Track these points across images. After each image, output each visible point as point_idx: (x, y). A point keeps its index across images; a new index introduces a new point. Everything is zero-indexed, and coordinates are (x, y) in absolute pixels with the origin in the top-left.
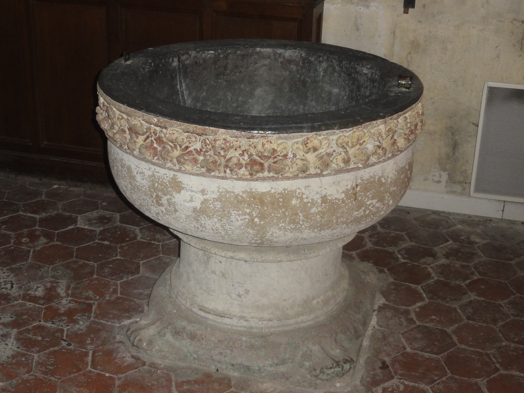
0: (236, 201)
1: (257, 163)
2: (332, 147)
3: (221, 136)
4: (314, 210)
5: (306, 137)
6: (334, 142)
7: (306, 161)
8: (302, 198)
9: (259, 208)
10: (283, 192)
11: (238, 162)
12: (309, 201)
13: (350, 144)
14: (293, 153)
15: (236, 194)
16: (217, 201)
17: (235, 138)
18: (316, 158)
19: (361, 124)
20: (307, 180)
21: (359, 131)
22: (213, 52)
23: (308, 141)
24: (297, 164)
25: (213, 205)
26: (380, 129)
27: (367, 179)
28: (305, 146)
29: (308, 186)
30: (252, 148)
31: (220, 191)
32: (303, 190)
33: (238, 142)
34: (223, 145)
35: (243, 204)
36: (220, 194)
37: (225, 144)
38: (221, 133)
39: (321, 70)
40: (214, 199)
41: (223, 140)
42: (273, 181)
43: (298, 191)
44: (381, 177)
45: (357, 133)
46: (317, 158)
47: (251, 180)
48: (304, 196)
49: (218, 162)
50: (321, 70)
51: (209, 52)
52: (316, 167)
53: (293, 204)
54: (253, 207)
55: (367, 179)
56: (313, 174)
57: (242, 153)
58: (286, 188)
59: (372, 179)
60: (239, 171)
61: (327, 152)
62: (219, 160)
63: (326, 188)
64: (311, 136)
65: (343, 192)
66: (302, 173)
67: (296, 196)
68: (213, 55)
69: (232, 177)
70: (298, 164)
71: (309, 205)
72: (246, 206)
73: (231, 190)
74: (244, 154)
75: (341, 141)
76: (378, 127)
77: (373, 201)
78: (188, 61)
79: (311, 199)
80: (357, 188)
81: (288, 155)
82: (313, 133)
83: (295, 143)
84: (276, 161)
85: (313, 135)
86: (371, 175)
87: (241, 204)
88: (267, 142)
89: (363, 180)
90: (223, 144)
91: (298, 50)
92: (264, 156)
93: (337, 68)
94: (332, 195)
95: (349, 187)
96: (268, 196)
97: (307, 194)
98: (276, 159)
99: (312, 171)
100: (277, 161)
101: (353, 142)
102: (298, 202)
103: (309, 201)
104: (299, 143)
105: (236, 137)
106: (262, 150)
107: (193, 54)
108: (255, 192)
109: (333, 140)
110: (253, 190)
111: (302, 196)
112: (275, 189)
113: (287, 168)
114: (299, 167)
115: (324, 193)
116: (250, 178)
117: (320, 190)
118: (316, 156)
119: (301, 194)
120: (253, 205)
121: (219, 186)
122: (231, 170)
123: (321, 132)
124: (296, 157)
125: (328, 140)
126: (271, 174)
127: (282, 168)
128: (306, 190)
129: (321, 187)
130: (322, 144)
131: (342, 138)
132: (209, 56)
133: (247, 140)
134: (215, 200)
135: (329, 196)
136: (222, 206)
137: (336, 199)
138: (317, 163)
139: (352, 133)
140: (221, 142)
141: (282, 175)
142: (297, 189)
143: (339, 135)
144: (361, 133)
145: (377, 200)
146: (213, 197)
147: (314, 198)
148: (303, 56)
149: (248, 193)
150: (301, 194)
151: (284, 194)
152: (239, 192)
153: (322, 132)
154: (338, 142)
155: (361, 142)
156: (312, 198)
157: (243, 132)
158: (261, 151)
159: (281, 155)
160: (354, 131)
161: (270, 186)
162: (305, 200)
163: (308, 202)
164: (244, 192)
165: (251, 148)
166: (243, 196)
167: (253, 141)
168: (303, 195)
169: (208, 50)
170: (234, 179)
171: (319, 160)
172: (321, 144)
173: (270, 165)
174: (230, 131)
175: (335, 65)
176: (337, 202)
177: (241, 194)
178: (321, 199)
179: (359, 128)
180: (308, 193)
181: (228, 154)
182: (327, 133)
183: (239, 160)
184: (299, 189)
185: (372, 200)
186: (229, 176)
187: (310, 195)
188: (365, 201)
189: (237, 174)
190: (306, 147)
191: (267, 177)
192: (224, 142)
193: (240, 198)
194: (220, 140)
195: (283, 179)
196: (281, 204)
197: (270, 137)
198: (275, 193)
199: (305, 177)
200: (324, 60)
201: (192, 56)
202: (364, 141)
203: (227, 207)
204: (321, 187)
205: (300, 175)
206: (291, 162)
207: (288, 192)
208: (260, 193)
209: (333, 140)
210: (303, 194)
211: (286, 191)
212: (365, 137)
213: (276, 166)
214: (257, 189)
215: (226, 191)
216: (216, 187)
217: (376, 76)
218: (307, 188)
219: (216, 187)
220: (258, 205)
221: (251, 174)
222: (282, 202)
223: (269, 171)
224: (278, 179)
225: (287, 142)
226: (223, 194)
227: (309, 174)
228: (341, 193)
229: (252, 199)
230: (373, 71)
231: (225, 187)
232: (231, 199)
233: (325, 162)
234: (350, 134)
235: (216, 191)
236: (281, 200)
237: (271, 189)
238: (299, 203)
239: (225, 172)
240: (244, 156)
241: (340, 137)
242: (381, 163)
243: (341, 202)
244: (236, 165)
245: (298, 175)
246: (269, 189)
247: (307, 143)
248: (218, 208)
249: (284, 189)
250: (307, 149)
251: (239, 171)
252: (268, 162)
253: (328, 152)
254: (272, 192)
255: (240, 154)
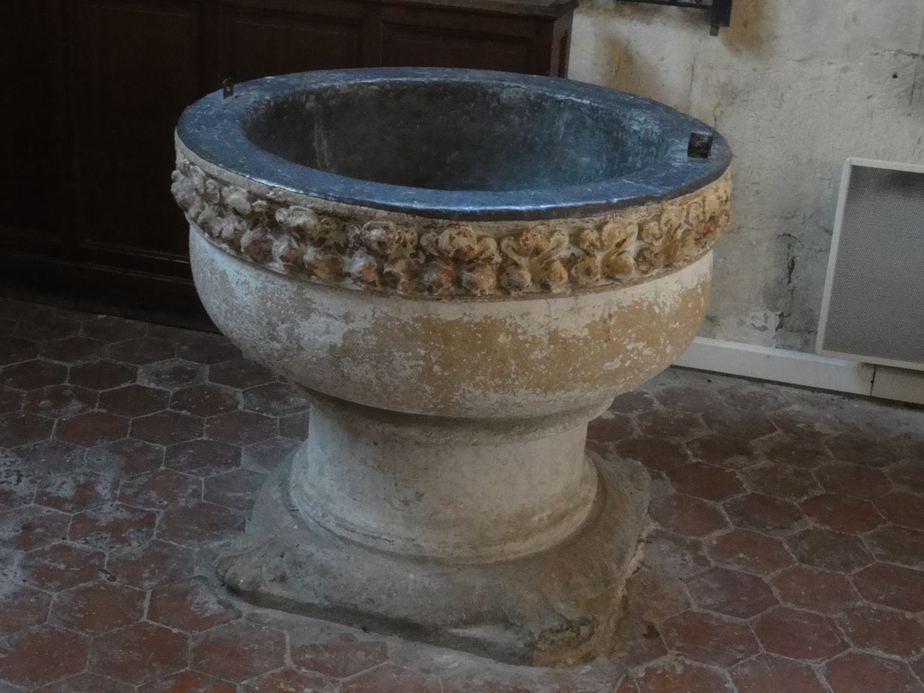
4: (536, 355)
8: (514, 334)
10: (483, 322)
15: (403, 322)
16: (370, 333)
27: (628, 306)
29: (528, 314)
31: (377, 315)
32: (518, 320)
36: (375, 322)
40: (365, 329)
44: (654, 304)
48: (520, 331)
55: (629, 306)
59: (637, 307)
63: (558, 318)
65: (588, 326)
71: (527, 345)
77: (638, 344)
79: (530, 335)
80: (610, 320)
86: (636, 299)
89: (621, 308)
94: (567, 330)
95: (597, 318)
102: (510, 339)
112: (470, 317)
115: (553, 326)
117: (547, 320)
120: (432, 343)
129: (548, 316)
135: (563, 332)
137: (574, 337)
145: (644, 344)
148: (531, 98)
150: (513, 326)
152: (408, 319)
156: (532, 334)
162: (521, 338)
163: (526, 341)
164: (415, 320)
176: (576, 342)
177: (411, 323)
178: (548, 336)
184: (511, 317)
185: (637, 342)
188: (624, 343)
193: (410, 330)
197: (463, 225)
198: (470, 323)
204: (548, 316)
207: (492, 321)
210: (518, 326)
211: (489, 321)
218: (524, 317)
228: (584, 327)
229: (431, 333)
242: (654, 279)
243: (582, 344)
246: (460, 315)
249: (486, 317)
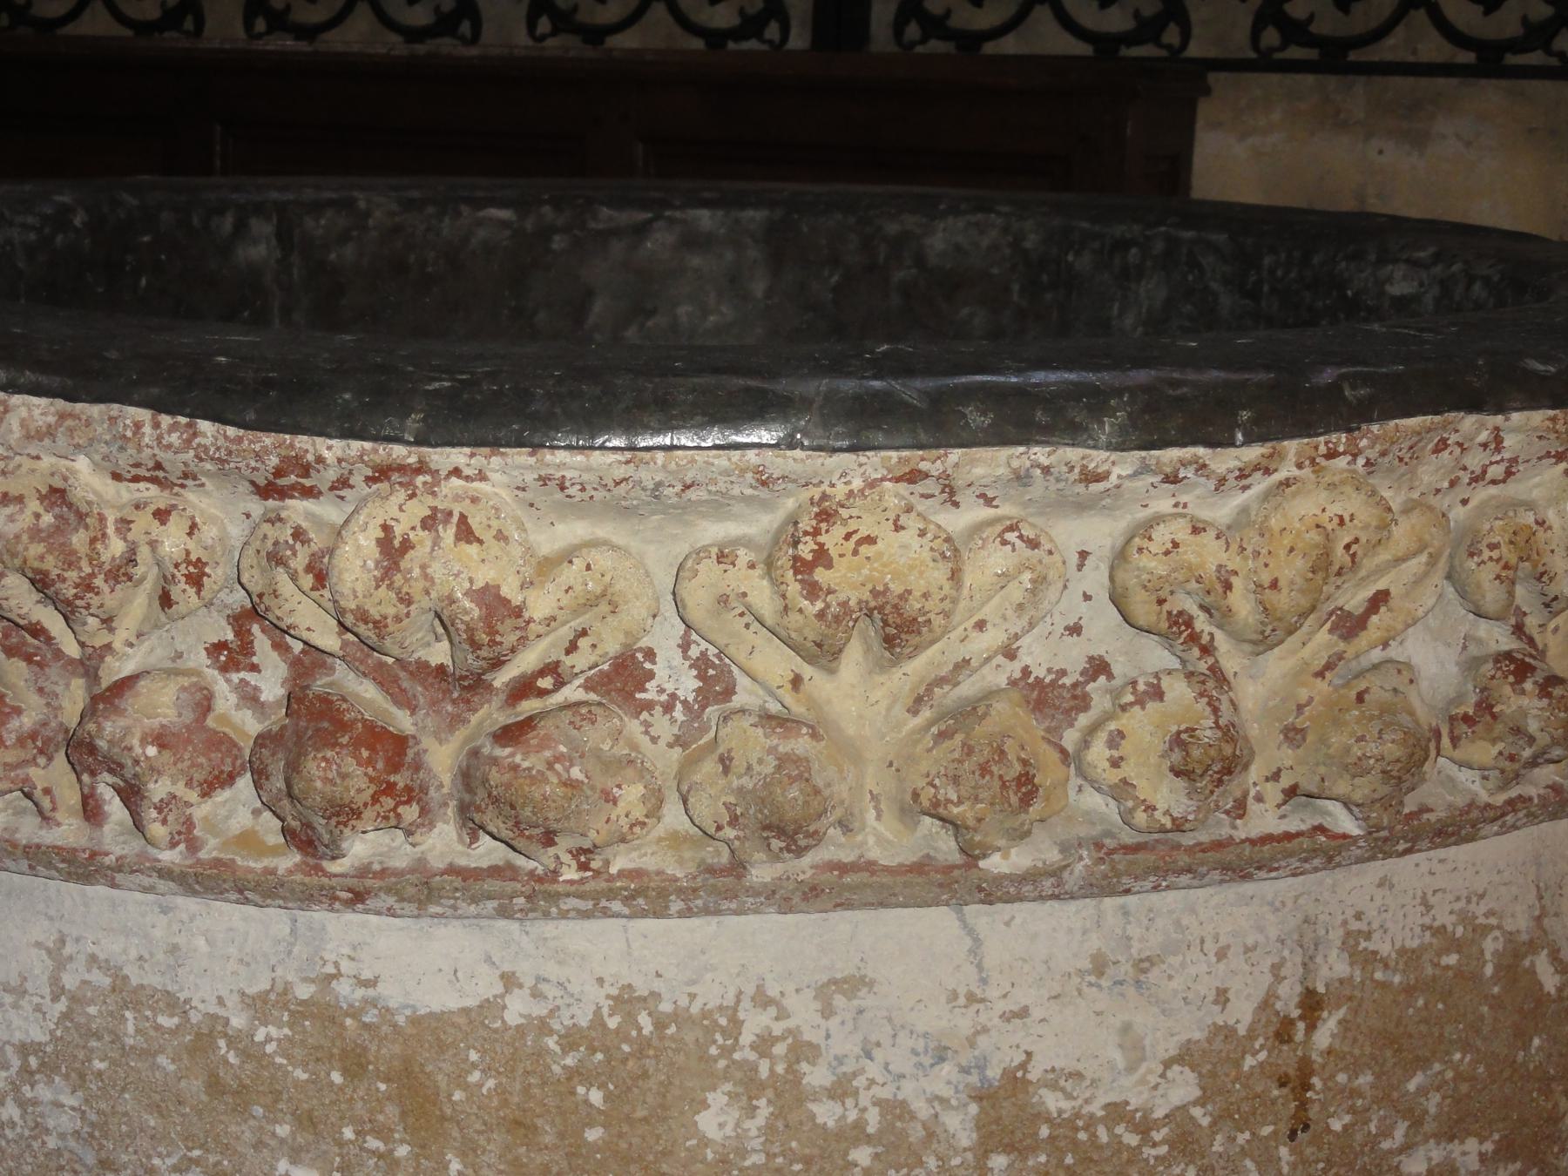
0: (194, 1086)
1: (344, 726)
2: (1075, 630)
3: (27, 464)
5: (805, 495)
6: (1096, 578)
7: (814, 735)
8: (790, 1093)
9: (396, 1163)
10: (613, 1023)
11: (189, 717)
12: (859, 1125)
13: (1242, 603)
14: (694, 652)
15: (195, 1017)
16: (49, 1068)
17: (154, 490)
18: (914, 711)
19: (1352, 417)
20: (842, 921)
21: (1331, 486)
22: (505, 214)
23: (832, 539)
24: (725, 763)
25: (22, 1104)
26: (1530, 506)
27: (1402, 951)
28: (794, 588)
29: (853, 984)
30: (294, 577)
31: (69, 981)
32: (804, 1014)
33: (176, 526)
34: (36, 549)
35: (258, 1111)
36: (65, 1016)
37: (55, 537)
38: (17, 432)
39: (1129, 321)
40: (24, 1049)
41: (42, 498)
42: (504, 913)
43: (755, 1022)
44: (1532, 947)
45: (1307, 507)
46: (926, 714)
47: (307, 898)
48: (817, 1076)
49: (18, 711)
50: (1129, 321)
51: (481, 214)
52: (916, 795)
53: (705, 1142)
54: (341, 1143)
55: (1411, 957)
56: (888, 870)
57: (230, 636)
58: (642, 991)
59: (1452, 959)
60: (202, 810)
61: (1026, 672)
62: (34, 699)
63: (1023, 1013)
64: (857, 483)
65: (1185, 1056)
66: (776, 844)
67: (740, 1065)
68: (507, 233)
69: (143, 856)
70: (739, 764)
71: (862, 1156)
72: (283, 1130)
73: (154, 980)
74: (247, 648)
75: (1158, 567)
76: (1512, 489)
77: (1456, 1148)
78: (349, 250)
79: (877, 1103)
80: (1311, 1028)
81: (650, 675)
82: (875, 463)
83: (699, 553)
84: (528, 724)
85: (872, 484)
86: (1443, 917)
87: (241, 1110)
88: (429, 523)
89: (1370, 959)
90: (35, 533)
91: (999, 213)
92: (423, 665)
93: (1227, 301)
94: (1078, 1075)
95: (1241, 1013)
96: (474, 1056)
97: (840, 1060)
98: (529, 706)
99: (881, 840)
100: (530, 719)
101: (1274, 585)
102: (760, 1120)
103: (859, 1125)
104: (744, 556)
105: (157, 475)
106: (383, 603)
107: (378, 214)
108: (355, 1013)
109: (1083, 555)
110: (344, 989)
111: (789, 1069)
112: (536, 994)
113: (631, 795)
114: (741, 791)
115: (1001, 1055)
116: (298, 877)
117: (964, 1023)
118: (919, 700)
119: (780, 1049)
120: (348, 1133)
121: (62, 941)
122: (131, 795)
123: (955, 455)
124: (729, 692)
125: (1033, 544)
126: (488, 852)
127: (570, 784)
128: (827, 1012)
129: (972, 998)
130: (968, 580)
131: (1162, 535)
132: (482, 233)
133: (257, 507)
134: (33, 1062)
135: (1054, 1086)
136: (93, 1117)
137: (1116, 1112)
138: (924, 766)
139: (1267, 496)
140: (26, 520)
141: (583, 856)
142: (746, 1003)
143: (1142, 514)
144: (1352, 504)
145: (1488, 1147)
146: (18, 1036)
147: (908, 1090)
148: (1028, 245)
149: (302, 1012)
150: (780, 1049)
151: (627, 1039)
152: (221, 1001)
153: (973, 462)
154: (1128, 578)
155: (1354, 599)
156: (885, 1093)
157: (205, 426)
158: (375, 613)
159: (581, 660)
160: (1286, 483)
161: (489, 960)
162: (826, 1113)
163: (856, 1133)
164: (260, 1006)
165: (281, 576)
166: (260, 1036)
167: (309, 515)
168: (804, 1067)
169: (479, 204)
170: (165, 873)
171: (943, 736)
172: (955, 576)
173: (475, 753)
174: (96, 410)
175: (1214, 286)
176: (1132, 1140)
177: (238, 1022)
178: (974, 1108)
179: (1332, 455)
180: (852, 1047)
181: (117, 645)
182: (1021, 478)
183: (205, 704)
184: (763, 1000)
185: (1451, 1139)
186: (118, 851)
187: (873, 1070)
188: (1386, 1145)
189: (186, 836)
190: (813, 590)
191: (452, 870)
192: (48, 519)
193: (232, 1058)
194: (20, 499)
195: (596, 896)
196: (593, 1135)
197: (456, 472)
198: (543, 1027)
199: (812, 895)
200: (1149, 263)
201: (371, 222)
202: (1380, 600)
203: (131, 1135)
204: (972, 998)
205: (762, 873)
206: (678, 741)
207: (660, 1025)
208: (401, 1020)
209: (1083, 555)
210: (803, 1051)
211: (645, 1020)
212: (1384, 556)
213: (515, 768)
214: (371, 983)
215: (120, 983)
216: (38, 945)
217: (1477, 287)
218: (839, 1001)
219: (38, 945)
220: (383, 1133)
221: (302, 839)
222: (606, 1119)
223: (472, 828)
224: (554, 897)
225: (634, 544)
226: (92, 1010)
227: (843, 868)
228: (1167, 1064)
229: (337, 1077)
230: (1455, 268)
231: (111, 947)
232: (162, 1060)
233: (1002, 753)
234: (1244, 510)
235: (40, 984)
236: (596, 1097)
237: (499, 988)
238: (769, 1130)
239: (91, 811)
240: (254, 668)
241: (1146, 529)
242: (1533, 818)
243: (1164, 1150)
244: (162, 746)
245: (738, 867)
246: (486, 986)
247: (822, 557)
248: (62, 1136)
249: (626, 1001)
250: (821, 615)
251: (202, 810)
252: (461, 733)
253: (1039, 672)
254: (512, 1017)
255: (217, 648)
